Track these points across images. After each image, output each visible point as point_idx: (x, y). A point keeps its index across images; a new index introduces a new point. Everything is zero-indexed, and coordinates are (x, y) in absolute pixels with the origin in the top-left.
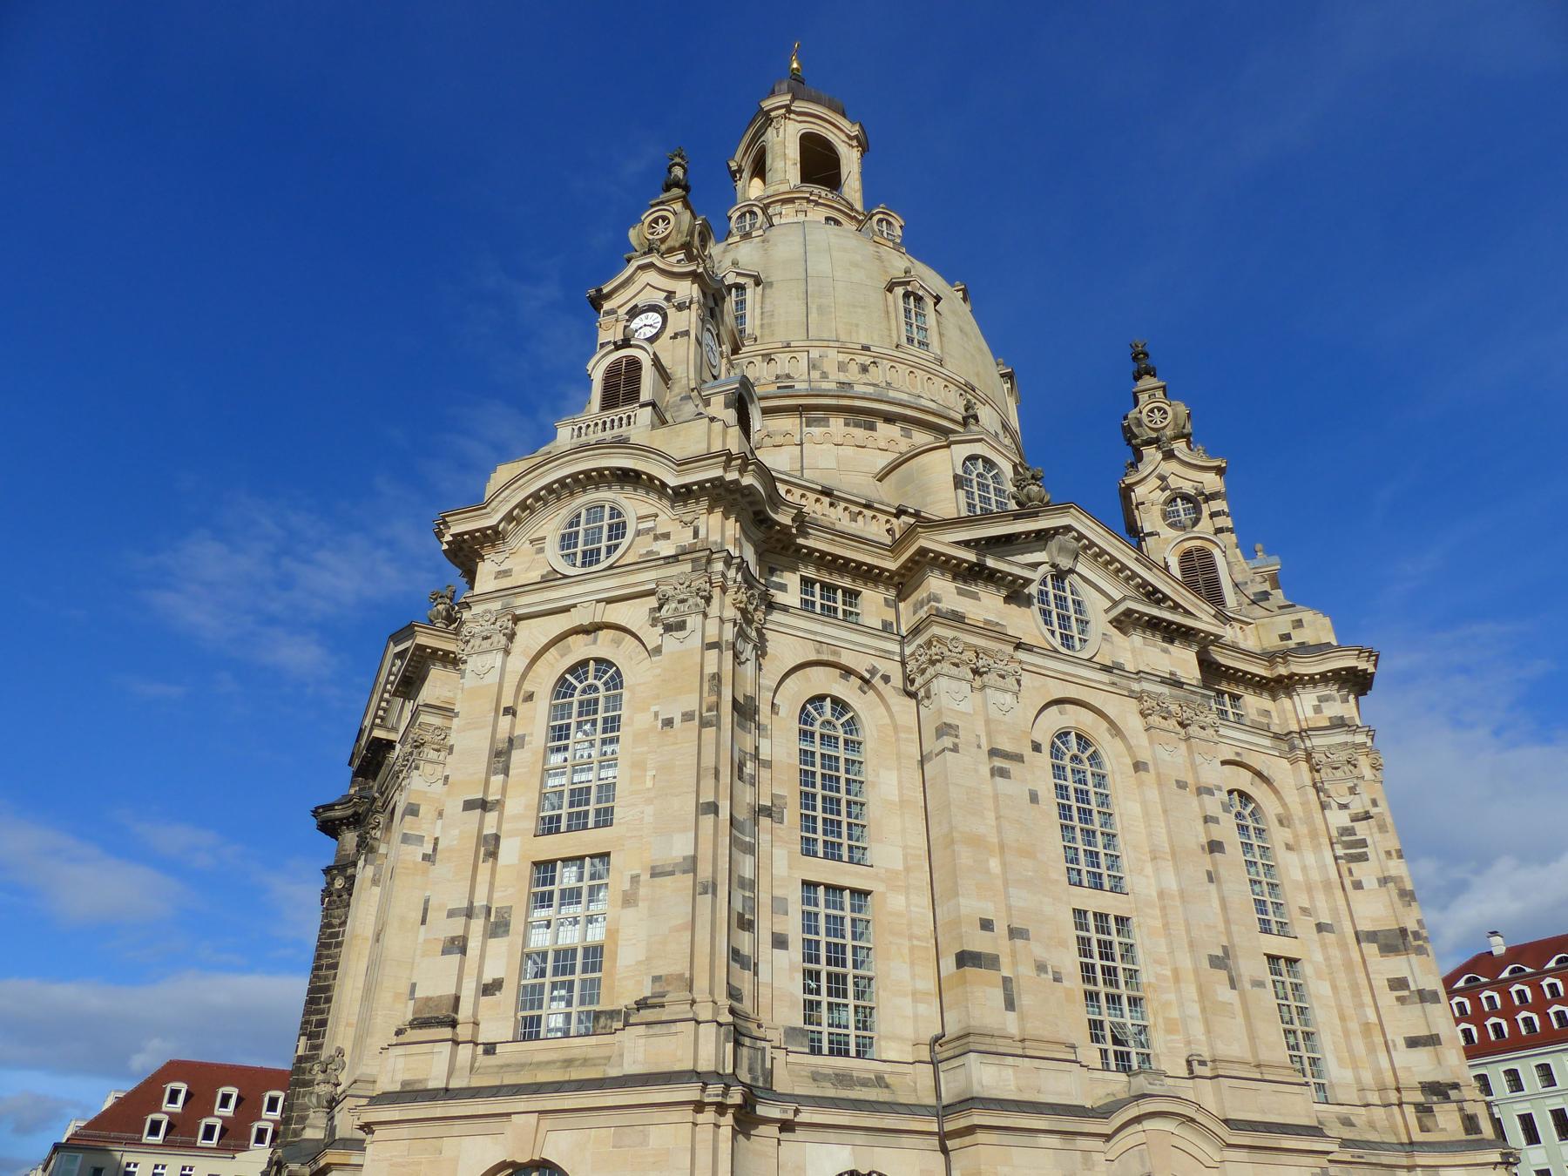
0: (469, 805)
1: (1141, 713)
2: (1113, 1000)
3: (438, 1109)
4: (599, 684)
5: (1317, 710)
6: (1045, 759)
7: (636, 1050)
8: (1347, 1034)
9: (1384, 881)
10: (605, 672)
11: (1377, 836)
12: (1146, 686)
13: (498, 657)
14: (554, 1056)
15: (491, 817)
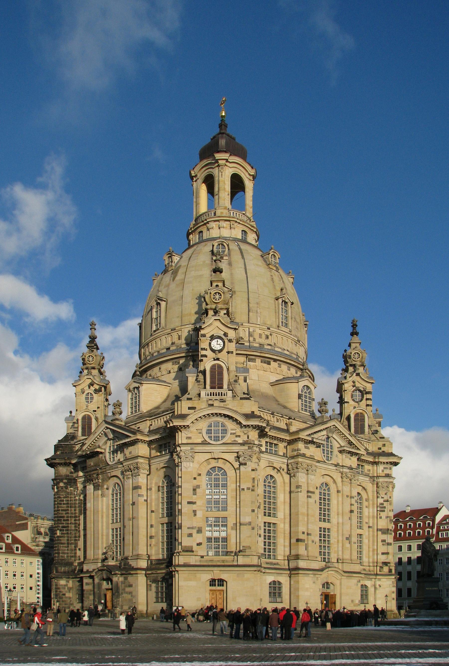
0: (189, 503)
1: (341, 477)
2: (325, 546)
3: (196, 568)
4: (220, 474)
5: (383, 471)
6: (317, 492)
7: (241, 560)
8: (369, 551)
9: (387, 517)
10: (221, 471)
11: (389, 506)
12: (344, 470)
13: (191, 464)
14: (219, 559)
15: (194, 505)
